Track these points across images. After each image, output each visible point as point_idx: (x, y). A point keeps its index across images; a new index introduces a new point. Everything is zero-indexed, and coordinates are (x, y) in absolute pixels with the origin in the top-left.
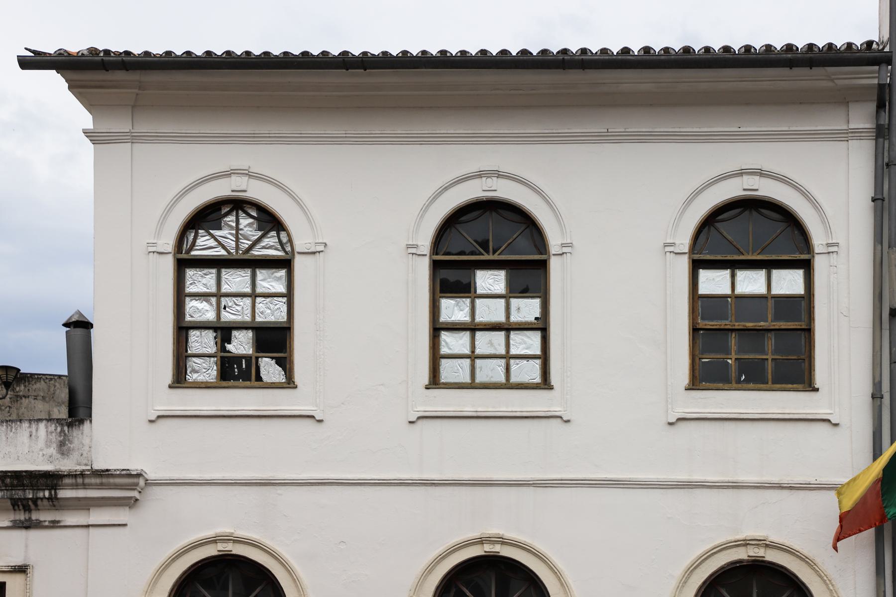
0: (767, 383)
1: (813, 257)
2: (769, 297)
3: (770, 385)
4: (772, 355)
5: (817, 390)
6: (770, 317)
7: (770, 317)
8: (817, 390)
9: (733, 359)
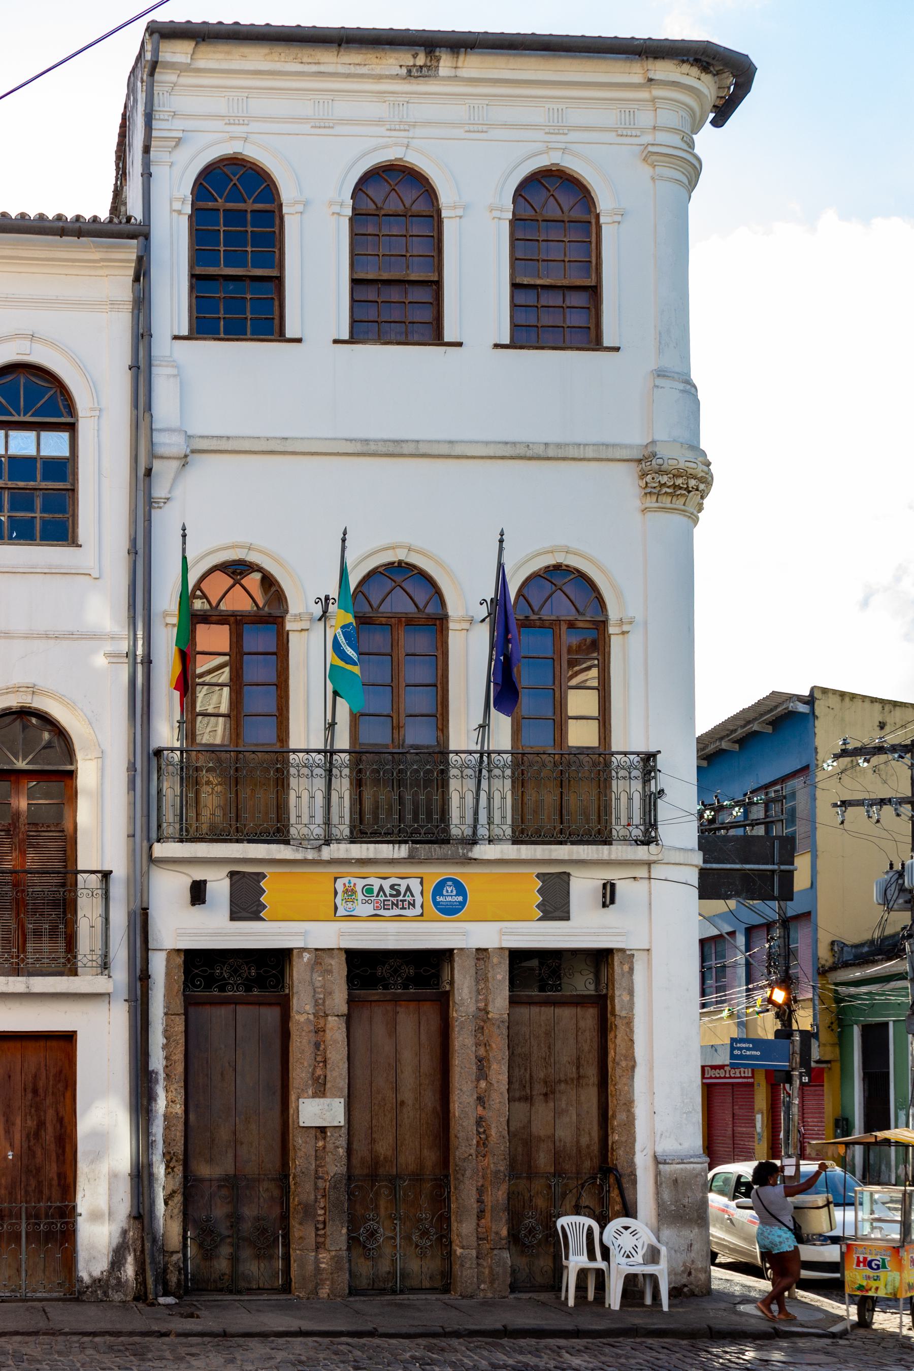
0: (36, 540)
1: (78, 420)
2: (38, 458)
3: (38, 541)
4: (41, 513)
5: (81, 546)
6: (39, 477)
7: (39, 477)
8: (81, 546)
9: (6, 517)
